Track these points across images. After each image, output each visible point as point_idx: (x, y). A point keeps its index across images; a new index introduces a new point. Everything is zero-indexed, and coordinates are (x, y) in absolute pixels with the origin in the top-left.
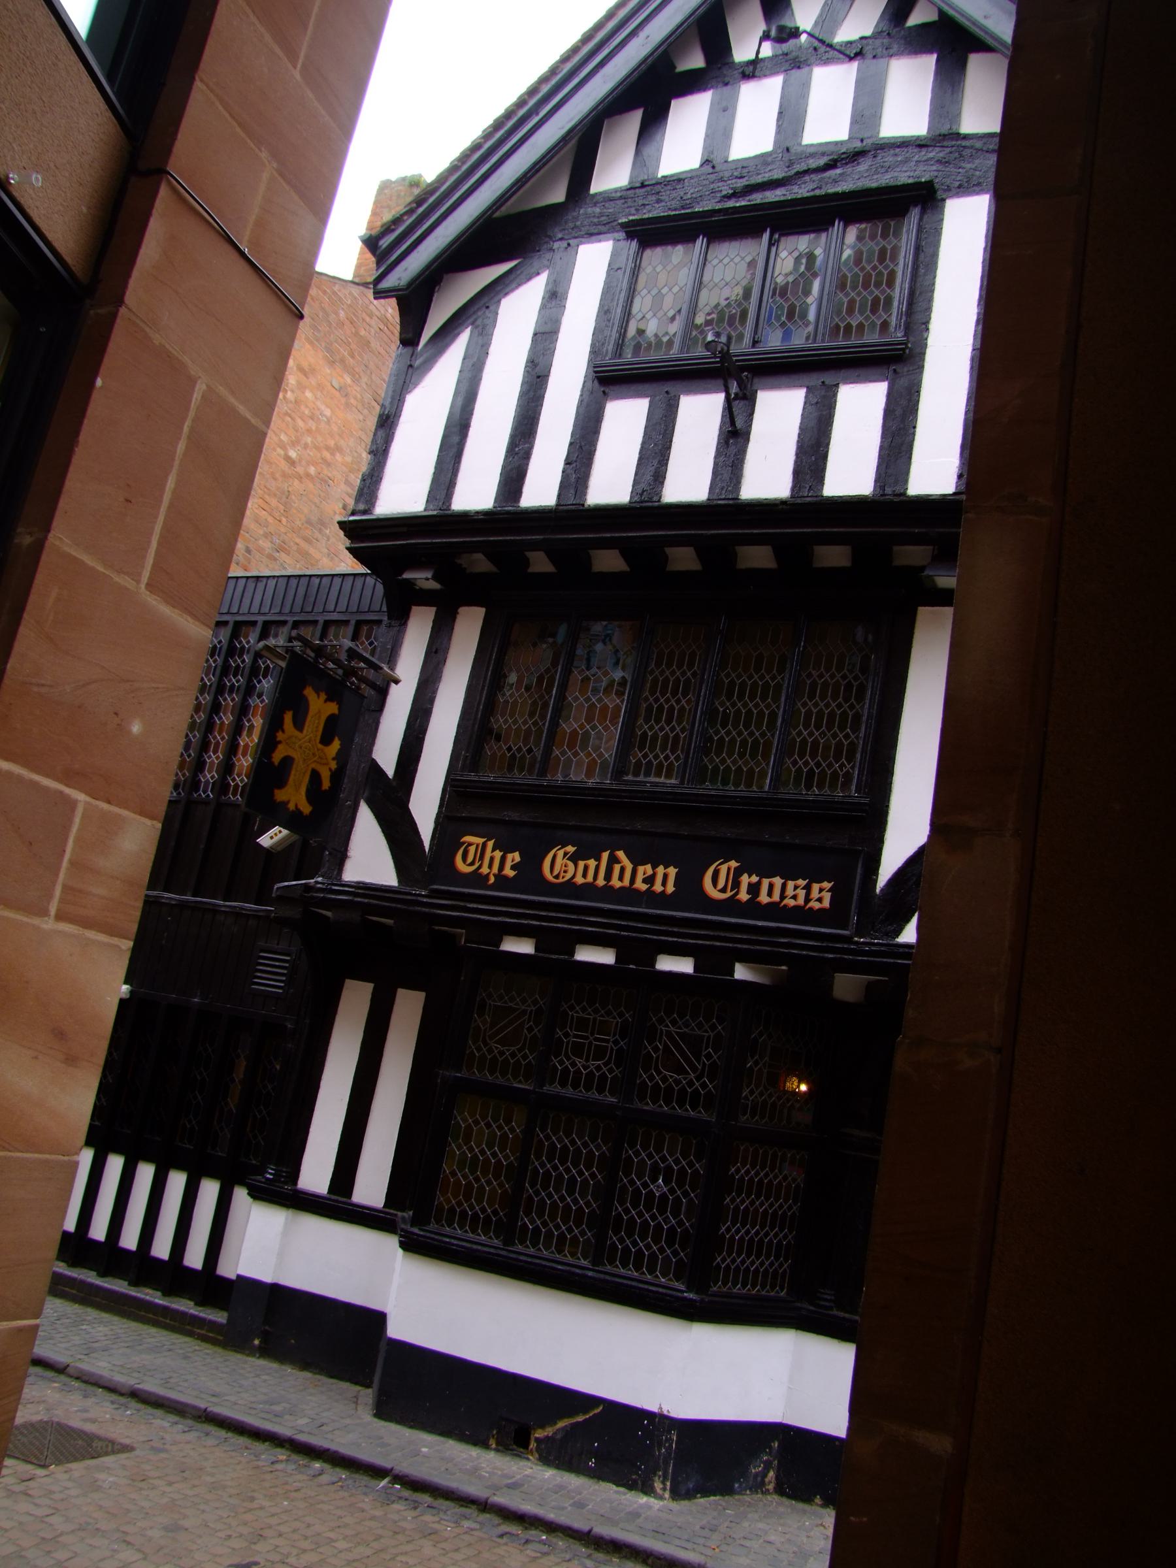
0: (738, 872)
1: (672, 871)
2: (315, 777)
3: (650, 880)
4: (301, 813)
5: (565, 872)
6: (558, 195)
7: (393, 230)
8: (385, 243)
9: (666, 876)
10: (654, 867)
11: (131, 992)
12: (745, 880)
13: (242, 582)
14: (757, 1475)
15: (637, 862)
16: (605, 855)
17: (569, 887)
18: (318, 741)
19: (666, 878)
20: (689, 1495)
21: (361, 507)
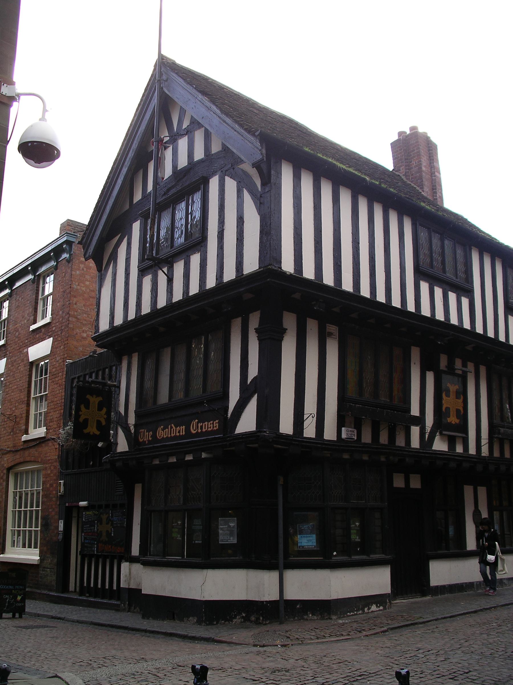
0: (198, 423)
1: (184, 427)
2: (99, 423)
3: (179, 432)
4: (96, 435)
5: (162, 435)
7: (85, 237)
9: (183, 429)
10: (180, 427)
11: (89, 504)
15: (176, 427)
16: (170, 426)
18: (97, 411)
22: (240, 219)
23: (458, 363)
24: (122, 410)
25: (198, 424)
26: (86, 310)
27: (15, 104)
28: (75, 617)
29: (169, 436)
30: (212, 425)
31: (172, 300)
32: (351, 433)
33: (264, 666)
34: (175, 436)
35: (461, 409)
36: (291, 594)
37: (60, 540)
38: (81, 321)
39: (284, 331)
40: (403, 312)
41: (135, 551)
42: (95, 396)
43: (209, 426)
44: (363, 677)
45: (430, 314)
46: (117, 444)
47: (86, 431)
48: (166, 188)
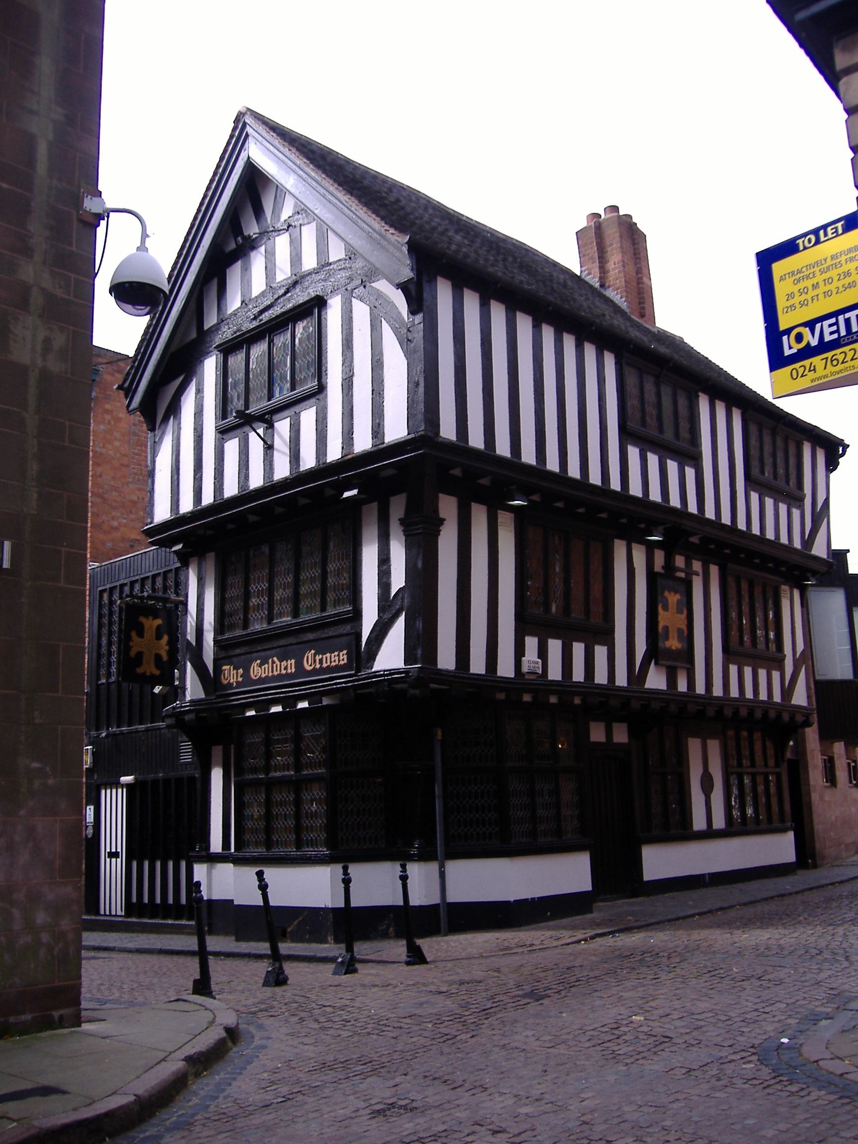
0: (315, 655)
1: (293, 661)
2: (158, 657)
3: (286, 668)
6: (194, 335)
8: (126, 385)
11: (136, 779)
12: (318, 658)
13: (140, 556)
15: (281, 661)
16: (270, 660)
17: (261, 680)
19: (290, 665)
21: (149, 521)
22: (377, 362)
23: (680, 561)
24: (191, 636)
26: (116, 485)
27: (103, 223)
28: (131, 945)
29: (270, 674)
30: (337, 658)
31: (273, 476)
33: (445, 979)
34: (280, 675)
35: (684, 627)
36: (455, 895)
37: (90, 836)
38: (110, 502)
39: (441, 521)
40: (604, 490)
41: (216, 844)
42: (151, 618)
43: (333, 660)
44: (581, 982)
45: (641, 492)
46: (184, 689)
47: (140, 670)
48: (258, 309)
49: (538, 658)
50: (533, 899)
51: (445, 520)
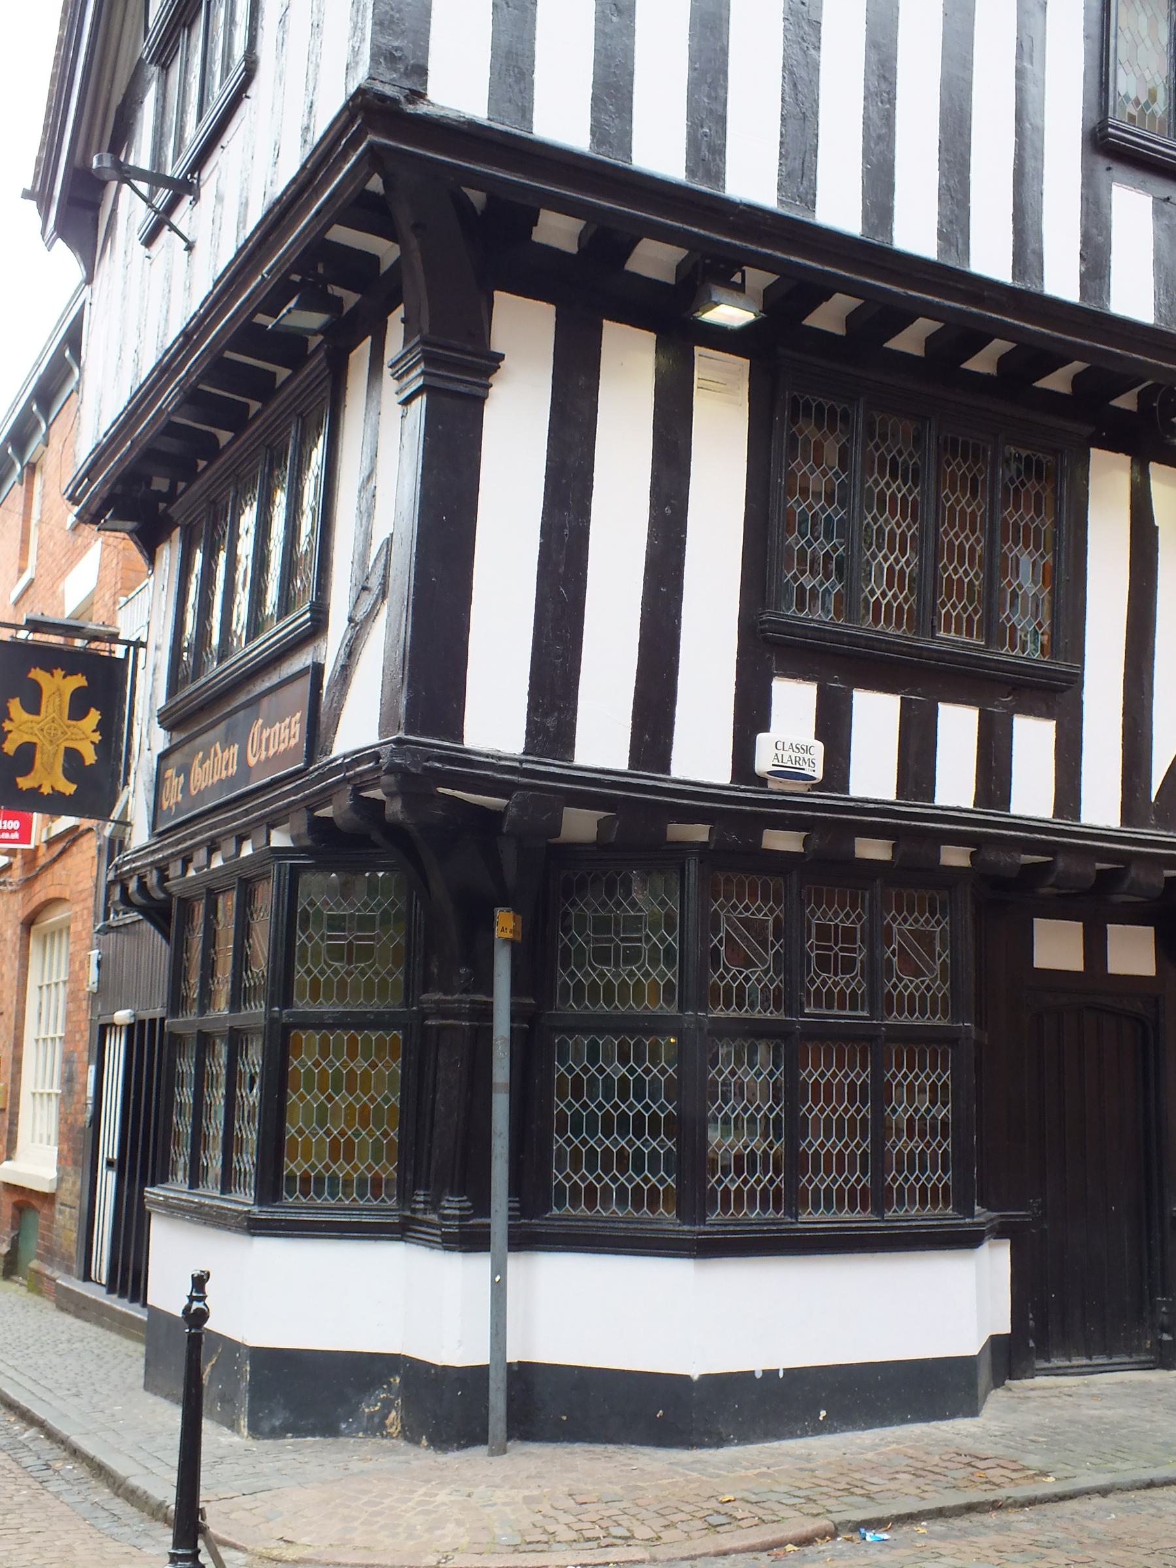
2: (72, 756)
4: (61, 795)
14: (372, 1416)
20: (276, 1433)
25: (262, 733)
32: (793, 755)
43: (282, 738)
49: (816, 738)
50: (770, 1374)
51: (501, 357)
